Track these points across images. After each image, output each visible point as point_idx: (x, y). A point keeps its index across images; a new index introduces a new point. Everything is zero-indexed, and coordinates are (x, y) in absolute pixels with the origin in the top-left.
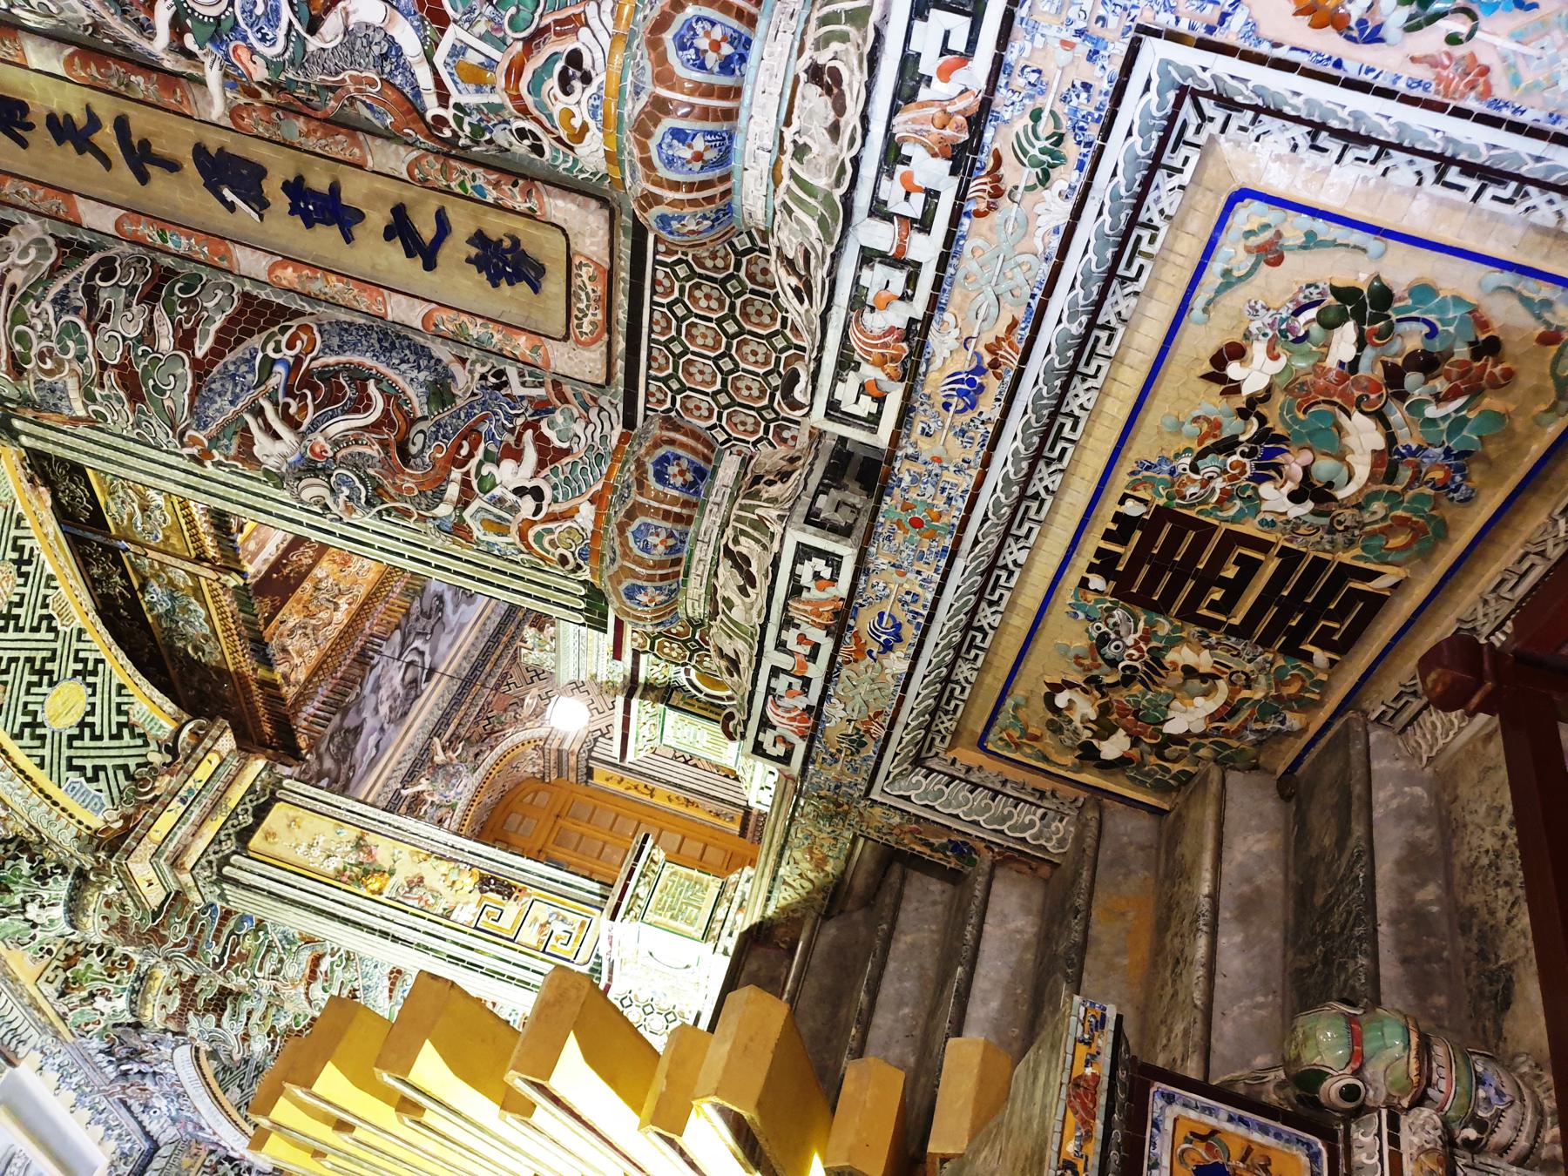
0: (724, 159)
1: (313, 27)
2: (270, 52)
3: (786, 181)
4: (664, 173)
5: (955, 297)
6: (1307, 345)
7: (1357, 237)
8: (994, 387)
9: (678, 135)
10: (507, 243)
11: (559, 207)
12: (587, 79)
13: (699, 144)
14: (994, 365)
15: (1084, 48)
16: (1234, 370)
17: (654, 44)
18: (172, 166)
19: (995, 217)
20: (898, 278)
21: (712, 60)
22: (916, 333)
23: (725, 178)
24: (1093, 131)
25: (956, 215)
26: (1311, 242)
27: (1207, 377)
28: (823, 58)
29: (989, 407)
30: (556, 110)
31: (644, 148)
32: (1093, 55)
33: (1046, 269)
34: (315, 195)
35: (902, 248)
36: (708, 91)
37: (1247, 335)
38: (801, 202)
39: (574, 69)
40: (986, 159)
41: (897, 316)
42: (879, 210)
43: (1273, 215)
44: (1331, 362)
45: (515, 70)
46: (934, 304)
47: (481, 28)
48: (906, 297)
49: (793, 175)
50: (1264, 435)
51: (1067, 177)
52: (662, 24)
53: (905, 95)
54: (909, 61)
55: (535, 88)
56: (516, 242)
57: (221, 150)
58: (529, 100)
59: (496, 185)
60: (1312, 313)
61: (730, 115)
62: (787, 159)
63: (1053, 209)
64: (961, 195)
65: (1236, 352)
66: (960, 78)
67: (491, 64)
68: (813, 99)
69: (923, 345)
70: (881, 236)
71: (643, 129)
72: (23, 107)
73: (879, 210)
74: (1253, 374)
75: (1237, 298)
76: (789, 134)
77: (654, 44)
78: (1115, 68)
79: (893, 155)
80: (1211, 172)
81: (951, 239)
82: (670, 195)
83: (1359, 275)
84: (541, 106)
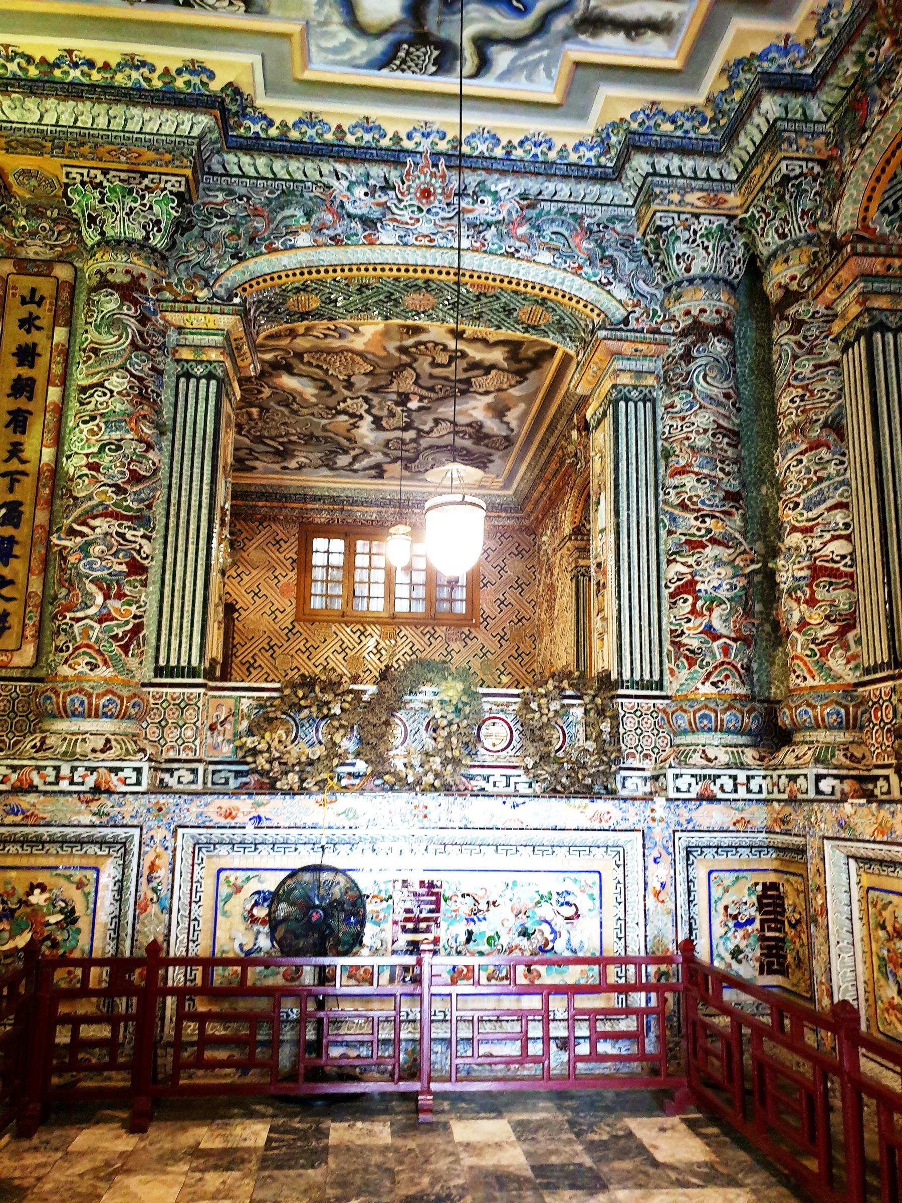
0: (74, 715)
1: (92, 581)
2: (81, 565)
3: (74, 738)
4: (68, 699)
5: (50, 798)
6: (51, 907)
7: (92, 906)
8: (18, 818)
9: (82, 703)
10: (7, 625)
11: (29, 650)
12: (91, 670)
13: (80, 709)
14: (27, 817)
15: (134, 814)
16: (37, 891)
17: (108, 692)
18: (11, 490)
19: (79, 804)
20: (51, 779)
21: (106, 710)
22: (32, 789)
23: (68, 716)
24: (112, 823)
25: (79, 793)
26: (87, 895)
27: (32, 884)
28: (114, 743)
29: (10, 819)
30: (79, 660)
31: (75, 691)
32: (132, 817)
33: (66, 822)
34: (11, 549)
35: (63, 778)
36: (97, 709)
37: (51, 890)
38: (69, 744)
39: (93, 666)
40: (97, 797)
41: (37, 780)
42: (74, 769)
43: (93, 881)
44: (47, 918)
45: (88, 646)
46: (45, 793)
47: (101, 636)
48: (45, 783)
49: (77, 740)
50: (13, 911)
51: (96, 820)
52: (114, 694)
53: (111, 770)
54: (121, 769)
55: (85, 653)
56: (9, 628)
57: (22, 513)
58: (81, 651)
59: (34, 625)
60: (63, 905)
61: (90, 716)
62: (80, 737)
63: (86, 819)
64: (85, 792)
65: (43, 888)
66: (119, 784)
67: (90, 639)
68: (100, 743)
69: (29, 792)
70: (65, 771)
71: (81, 690)
72: (23, 432)
73: (74, 769)
74: (38, 898)
75: (62, 882)
76: (88, 735)
77: (108, 692)
78: (130, 823)
79: (93, 770)
80: (102, 859)
81: (70, 793)
82: (61, 700)
83: (80, 910)
84: (79, 655)
